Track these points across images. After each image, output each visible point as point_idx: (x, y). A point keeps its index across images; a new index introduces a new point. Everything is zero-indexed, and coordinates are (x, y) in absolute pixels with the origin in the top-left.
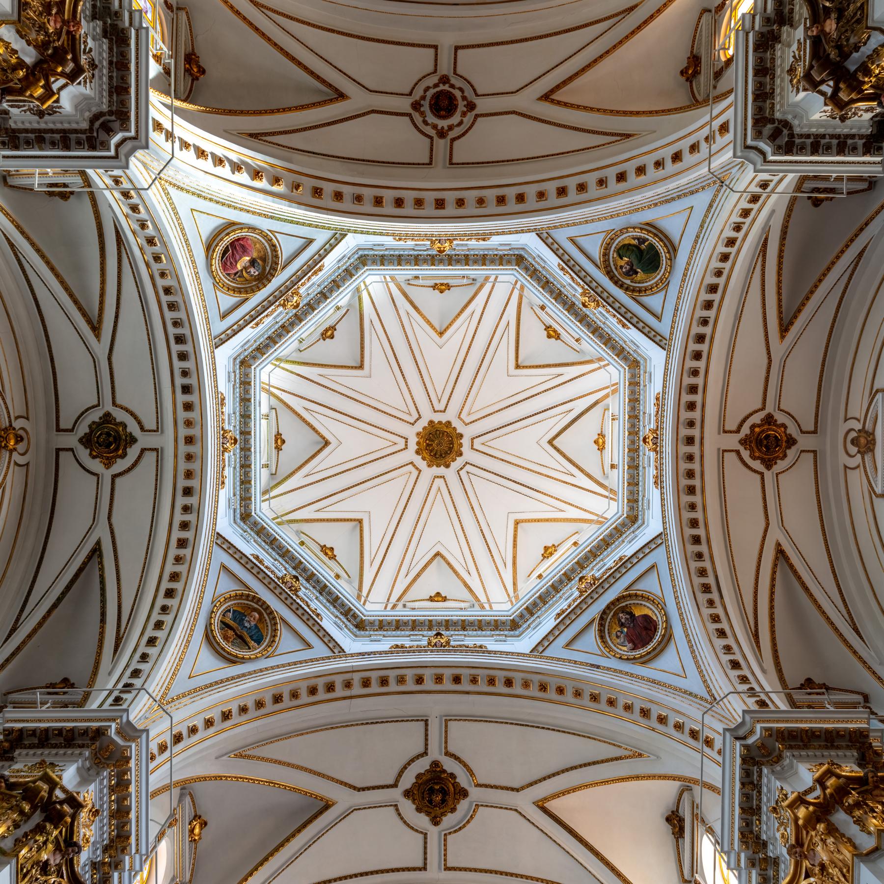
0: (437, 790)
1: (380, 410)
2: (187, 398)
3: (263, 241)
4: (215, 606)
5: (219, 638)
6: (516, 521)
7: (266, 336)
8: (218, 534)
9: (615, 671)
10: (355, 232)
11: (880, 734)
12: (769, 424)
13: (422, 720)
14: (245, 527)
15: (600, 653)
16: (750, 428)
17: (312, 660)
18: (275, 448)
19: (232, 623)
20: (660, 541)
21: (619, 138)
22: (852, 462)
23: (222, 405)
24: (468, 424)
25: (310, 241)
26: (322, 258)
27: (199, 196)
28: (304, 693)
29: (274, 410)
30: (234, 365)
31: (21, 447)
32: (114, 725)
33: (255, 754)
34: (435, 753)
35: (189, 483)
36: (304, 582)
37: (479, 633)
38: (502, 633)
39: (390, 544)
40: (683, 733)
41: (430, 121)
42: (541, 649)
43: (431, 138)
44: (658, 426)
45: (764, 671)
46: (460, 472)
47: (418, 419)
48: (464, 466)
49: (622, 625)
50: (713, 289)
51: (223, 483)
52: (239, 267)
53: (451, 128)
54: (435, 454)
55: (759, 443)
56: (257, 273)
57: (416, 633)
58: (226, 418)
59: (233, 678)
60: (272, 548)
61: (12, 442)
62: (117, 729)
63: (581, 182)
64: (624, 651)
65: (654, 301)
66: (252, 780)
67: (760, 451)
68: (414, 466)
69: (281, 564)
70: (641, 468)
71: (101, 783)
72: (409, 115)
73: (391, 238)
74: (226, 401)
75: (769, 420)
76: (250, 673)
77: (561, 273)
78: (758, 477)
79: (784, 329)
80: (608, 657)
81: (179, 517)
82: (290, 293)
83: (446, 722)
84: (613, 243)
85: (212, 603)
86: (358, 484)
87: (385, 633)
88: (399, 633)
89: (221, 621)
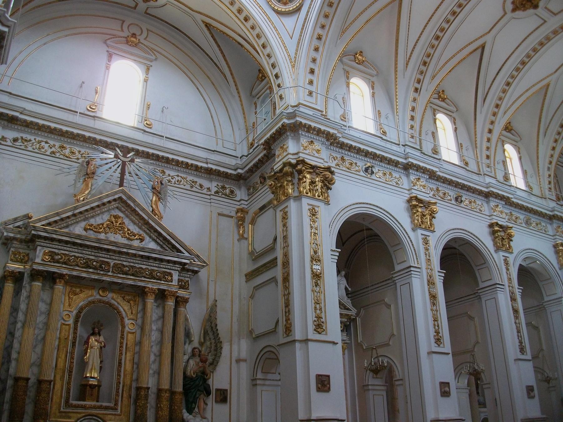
61: (134, 40)
71: (302, 135)
76: (309, 8)
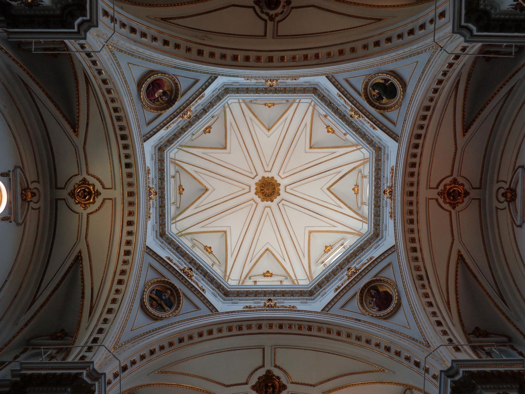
0: (270, 386)
1: (236, 171)
2: (129, 170)
3: (170, 81)
4: (146, 288)
5: (148, 306)
6: (309, 231)
7: (172, 134)
8: (147, 246)
9: (369, 323)
10: (223, 75)
11: (522, 362)
12: (455, 184)
13: (261, 348)
14: (162, 240)
15: (360, 312)
16: (444, 186)
17: (200, 317)
18: (179, 193)
19: (155, 297)
20: (394, 250)
21: (374, 21)
22: (501, 206)
23: (148, 173)
24: (283, 178)
25: (197, 81)
26: (204, 90)
27: (132, 55)
28: (196, 336)
29: (178, 173)
30: (155, 150)
31: (35, 199)
32: (85, 372)
33: (169, 370)
34: (268, 366)
35: (130, 218)
36: (195, 270)
37: (292, 298)
38: (304, 298)
39: (241, 244)
40: (410, 362)
41: (265, 11)
42: (327, 309)
43: (265, 21)
44: (392, 185)
45: (454, 325)
46: (279, 204)
47: (256, 176)
48: (281, 201)
49: (373, 297)
50: (427, 108)
51: (149, 217)
52: (156, 96)
53: (276, 15)
54: (265, 195)
55: (449, 194)
56: (167, 99)
57: (257, 298)
58: (151, 181)
59: (156, 329)
60: (178, 252)
61: (30, 196)
62: (87, 374)
63: (352, 46)
64: (374, 312)
65: (392, 114)
66: (168, 384)
67: (449, 199)
68: (254, 201)
69: (183, 261)
70: (381, 207)
72: (253, 8)
73: (243, 79)
74: (151, 171)
75: (455, 181)
76: (165, 326)
77: (339, 98)
78: (448, 214)
79: (466, 130)
80: (365, 315)
81: (125, 238)
82: (185, 110)
83: (275, 347)
84: (370, 82)
85: (144, 286)
86: (224, 212)
87: (240, 298)
88: (248, 298)
89: (149, 296)
